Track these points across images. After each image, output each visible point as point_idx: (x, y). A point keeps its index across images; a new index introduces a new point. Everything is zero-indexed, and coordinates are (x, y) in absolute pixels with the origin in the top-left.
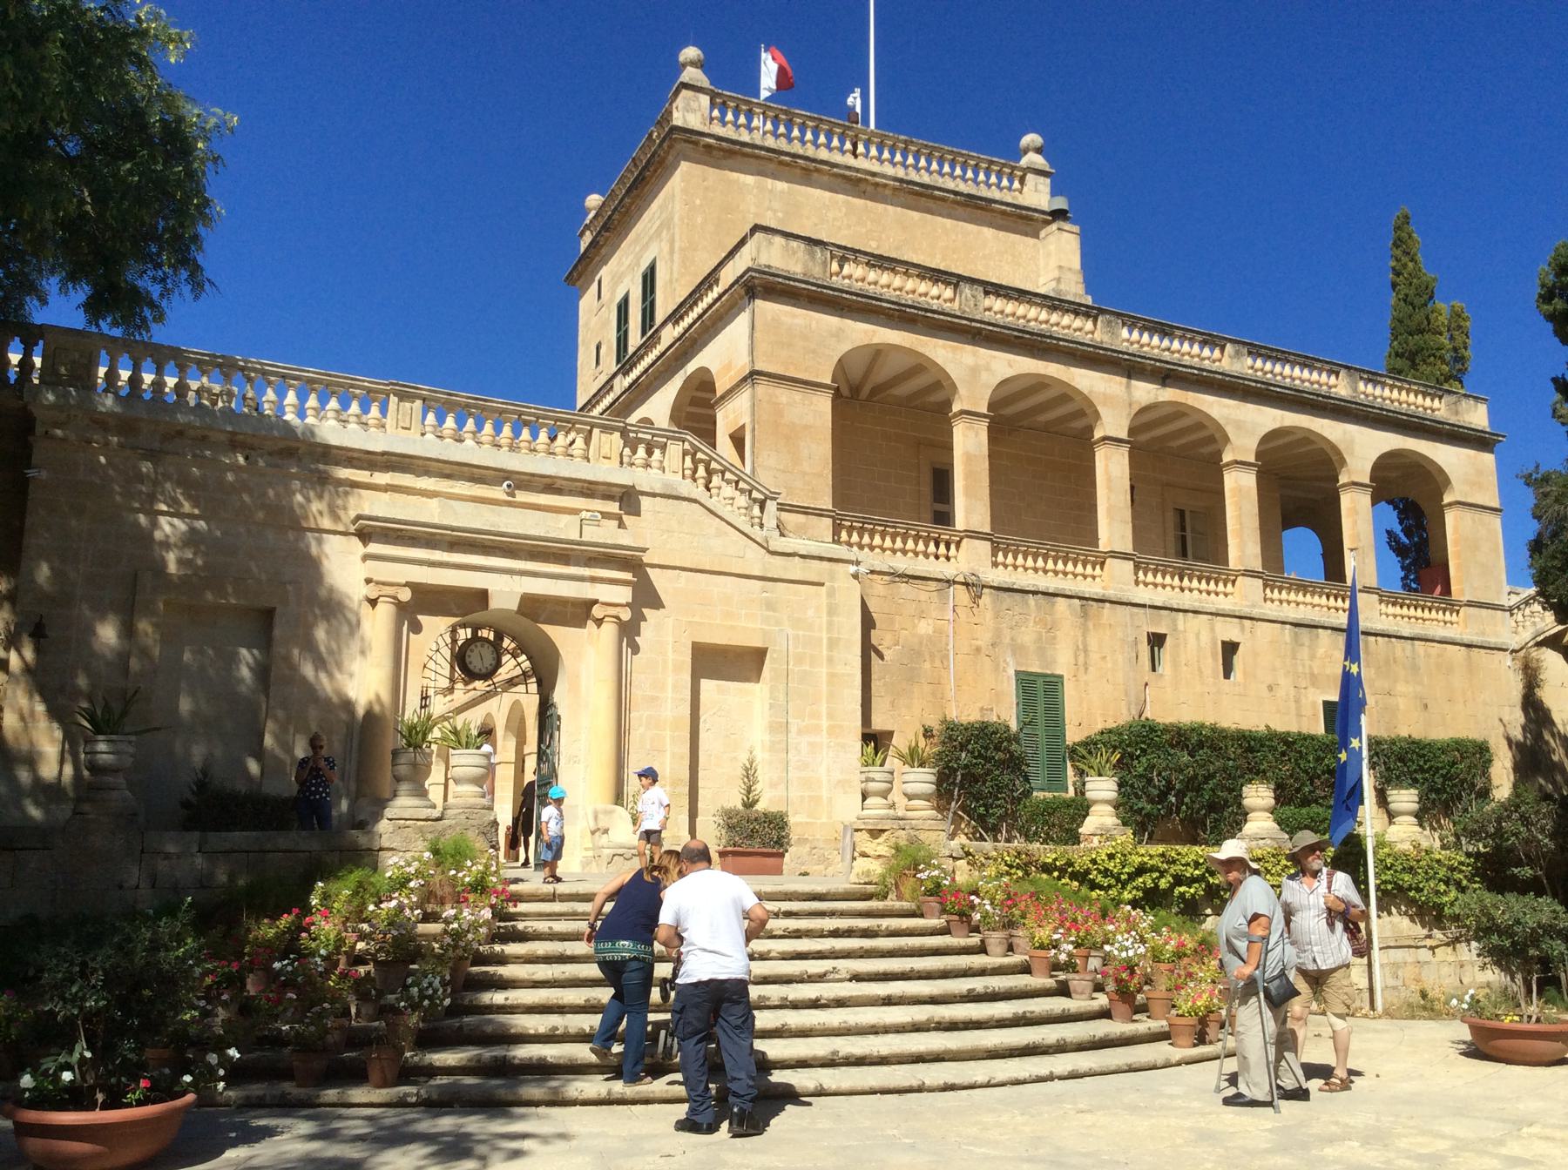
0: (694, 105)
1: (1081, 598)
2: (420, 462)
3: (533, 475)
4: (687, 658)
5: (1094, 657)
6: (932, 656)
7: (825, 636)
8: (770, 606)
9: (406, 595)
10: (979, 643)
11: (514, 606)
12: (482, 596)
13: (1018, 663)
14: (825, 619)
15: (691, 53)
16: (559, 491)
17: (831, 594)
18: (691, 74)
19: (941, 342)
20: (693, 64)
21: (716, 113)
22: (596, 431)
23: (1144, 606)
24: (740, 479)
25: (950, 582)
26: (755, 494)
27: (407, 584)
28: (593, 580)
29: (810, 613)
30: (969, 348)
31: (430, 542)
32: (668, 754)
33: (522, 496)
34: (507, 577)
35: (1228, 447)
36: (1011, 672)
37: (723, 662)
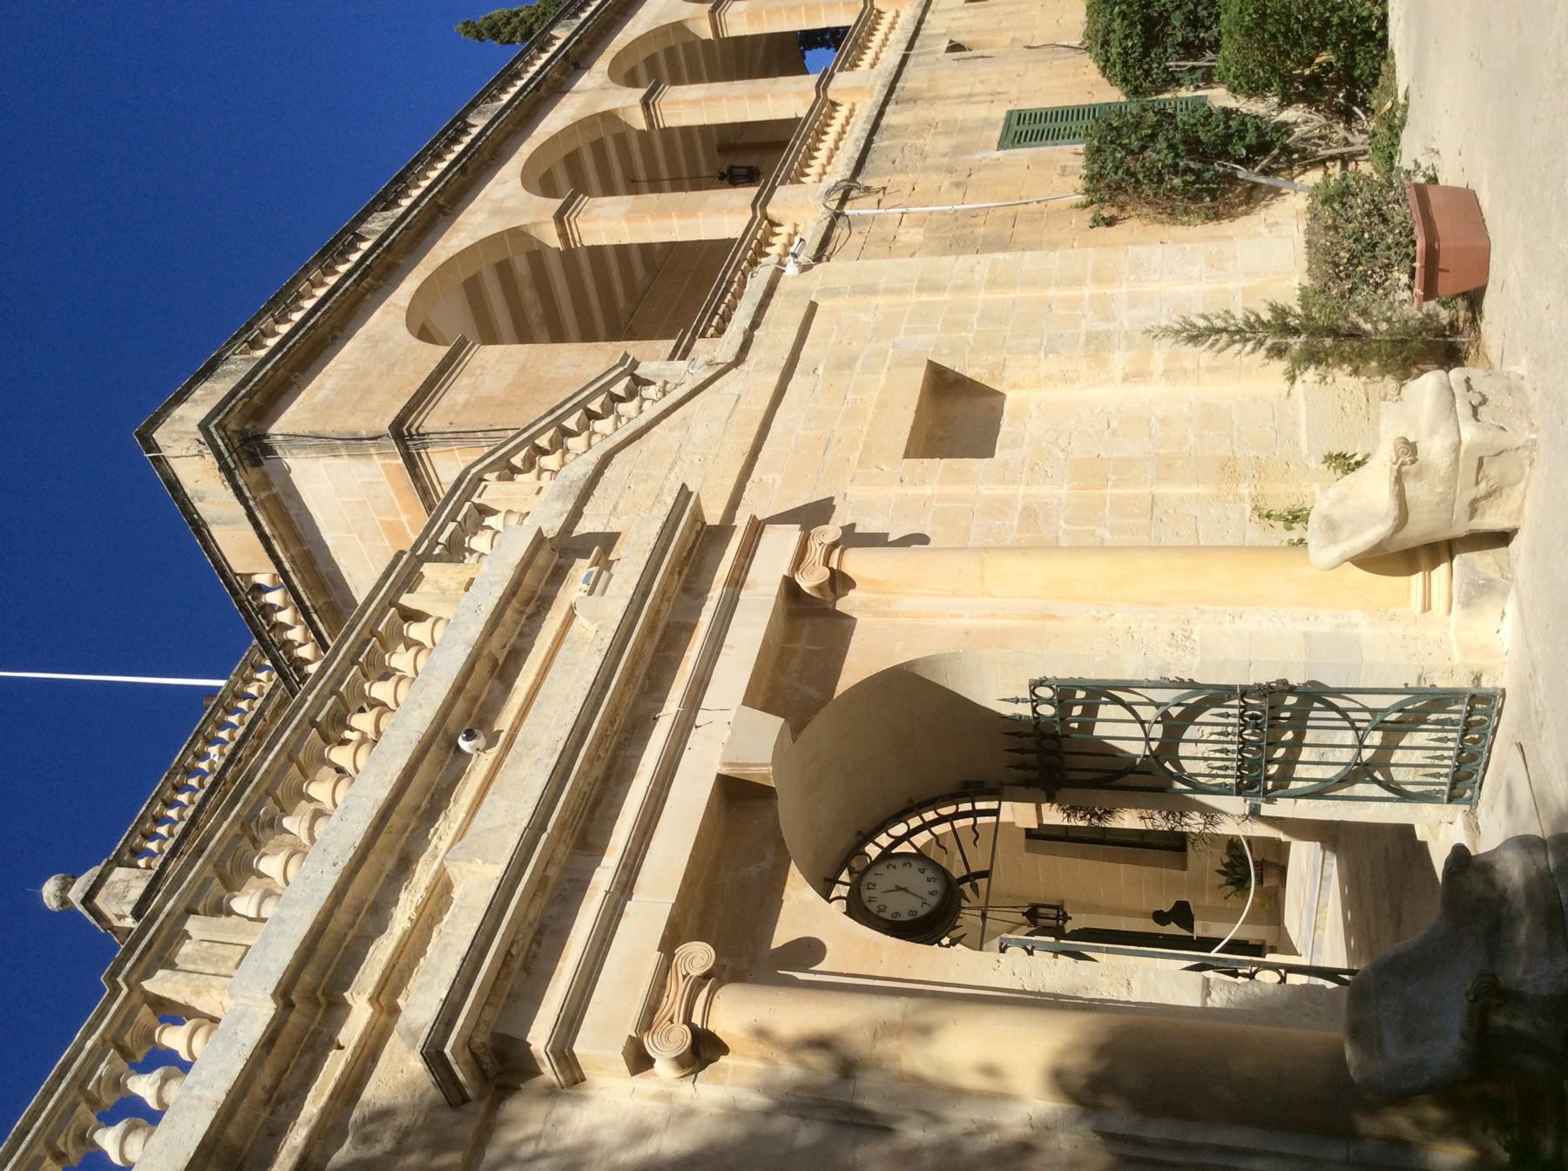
0: (120, 887)
1: (886, 102)
2: (342, 916)
3: (458, 690)
4: (940, 464)
5: (979, 88)
6: (964, 227)
7: (913, 299)
8: (844, 364)
9: (698, 956)
10: (946, 184)
11: (771, 726)
12: (736, 796)
13: (986, 148)
14: (880, 300)
15: (49, 891)
16: (516, 656)
17: (835, 292)
18: (76, 894)
19: (440, 243)
20: (64, 888)
21: (142, 863)
22: (406, 600)
23: (904, 60)
24: (582, 404)
25: (837, 215)
26: (619, 389)
27: (669, 944)
28: (737, 581)
29: (866, 318)
30: (461, 218)
31: (562, 894)
32: (1161, 490)
33: (505, 722)
34: (695, 738)
35: (690, 26)
36: (1001, 153)
37: (955, 414)
